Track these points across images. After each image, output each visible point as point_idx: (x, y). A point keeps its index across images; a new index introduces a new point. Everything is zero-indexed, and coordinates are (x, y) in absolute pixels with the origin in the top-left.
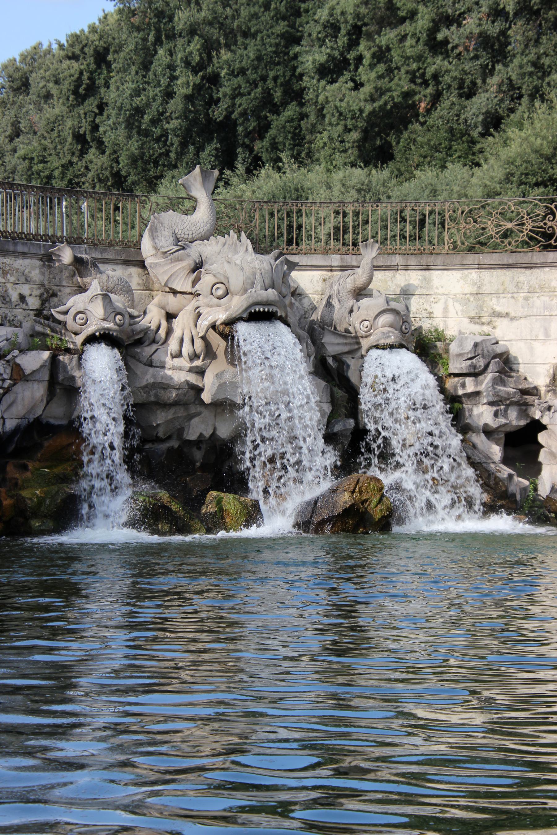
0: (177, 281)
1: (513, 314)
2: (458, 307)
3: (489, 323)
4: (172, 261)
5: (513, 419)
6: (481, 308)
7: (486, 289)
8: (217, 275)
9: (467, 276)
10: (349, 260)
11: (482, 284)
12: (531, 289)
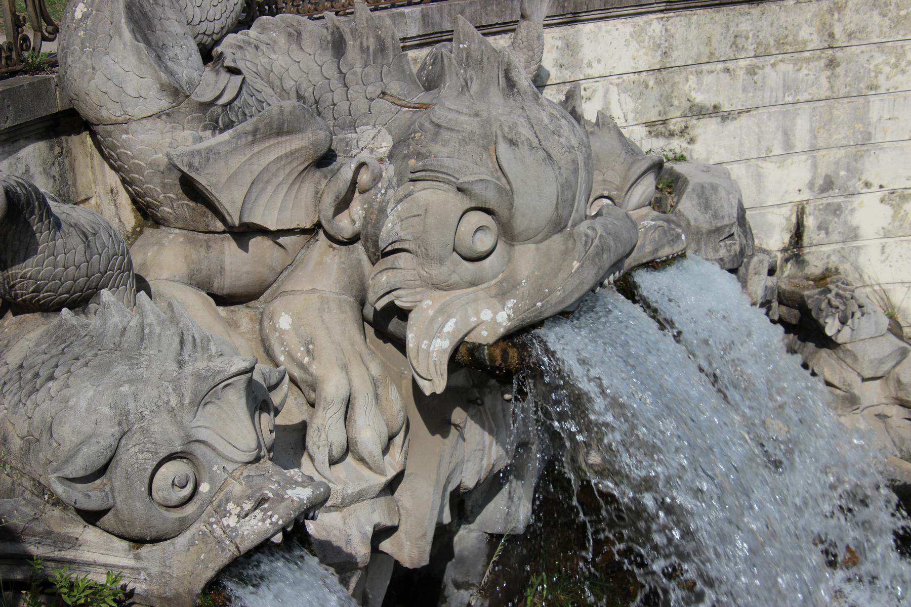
0: (264, 200)
1: (726, 107)
2: (630, 104)
3: (683, 132)
4: (256, 135)
6: (667, 100)
7: (679, 57)
8: (477, 189)
9: (642, 30)
10: (437, 18)
11: (670, 47)
12: (761, 49)
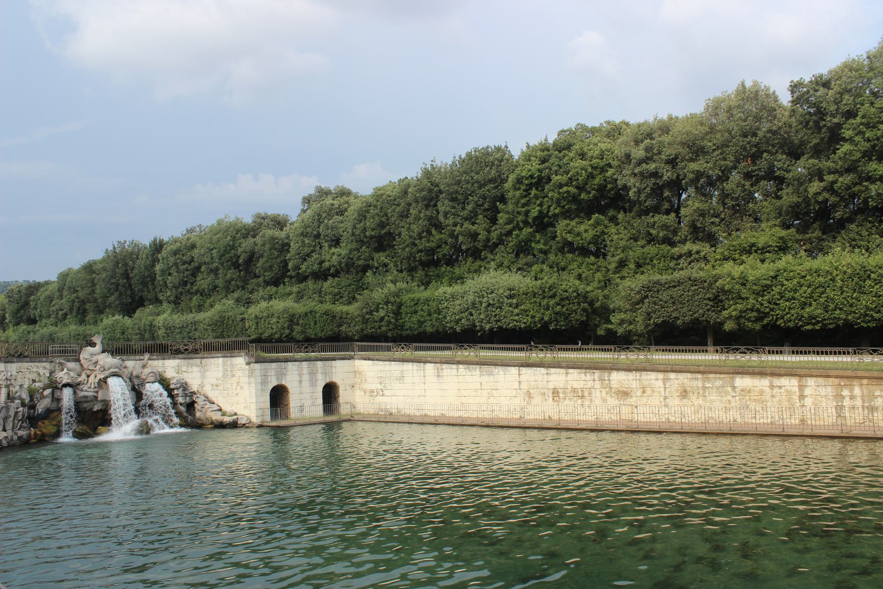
5: (188, 400)
